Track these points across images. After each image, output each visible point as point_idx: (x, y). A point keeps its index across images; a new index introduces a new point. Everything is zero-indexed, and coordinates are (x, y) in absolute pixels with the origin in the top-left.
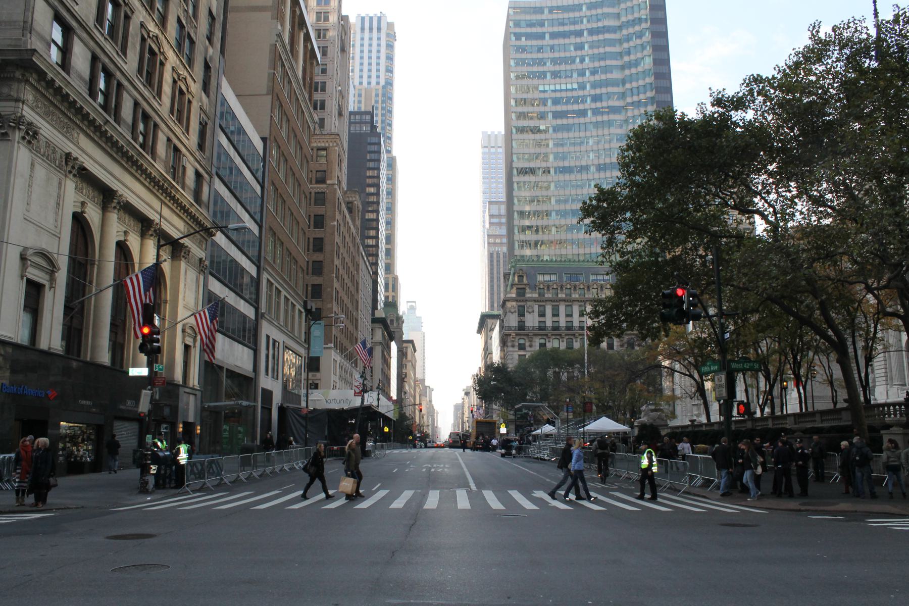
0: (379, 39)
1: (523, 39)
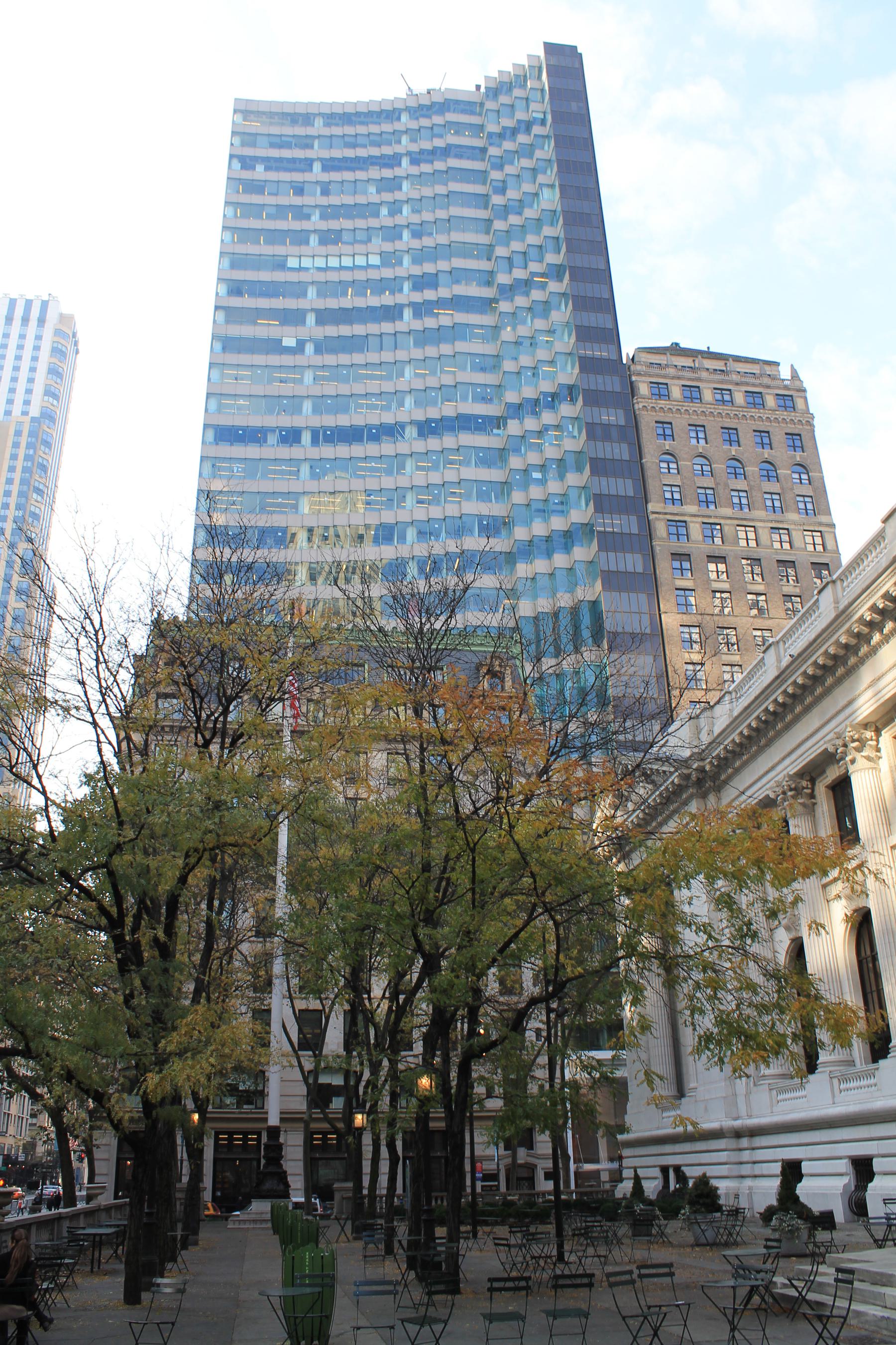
0: (39, 338)
1: (260, 168)
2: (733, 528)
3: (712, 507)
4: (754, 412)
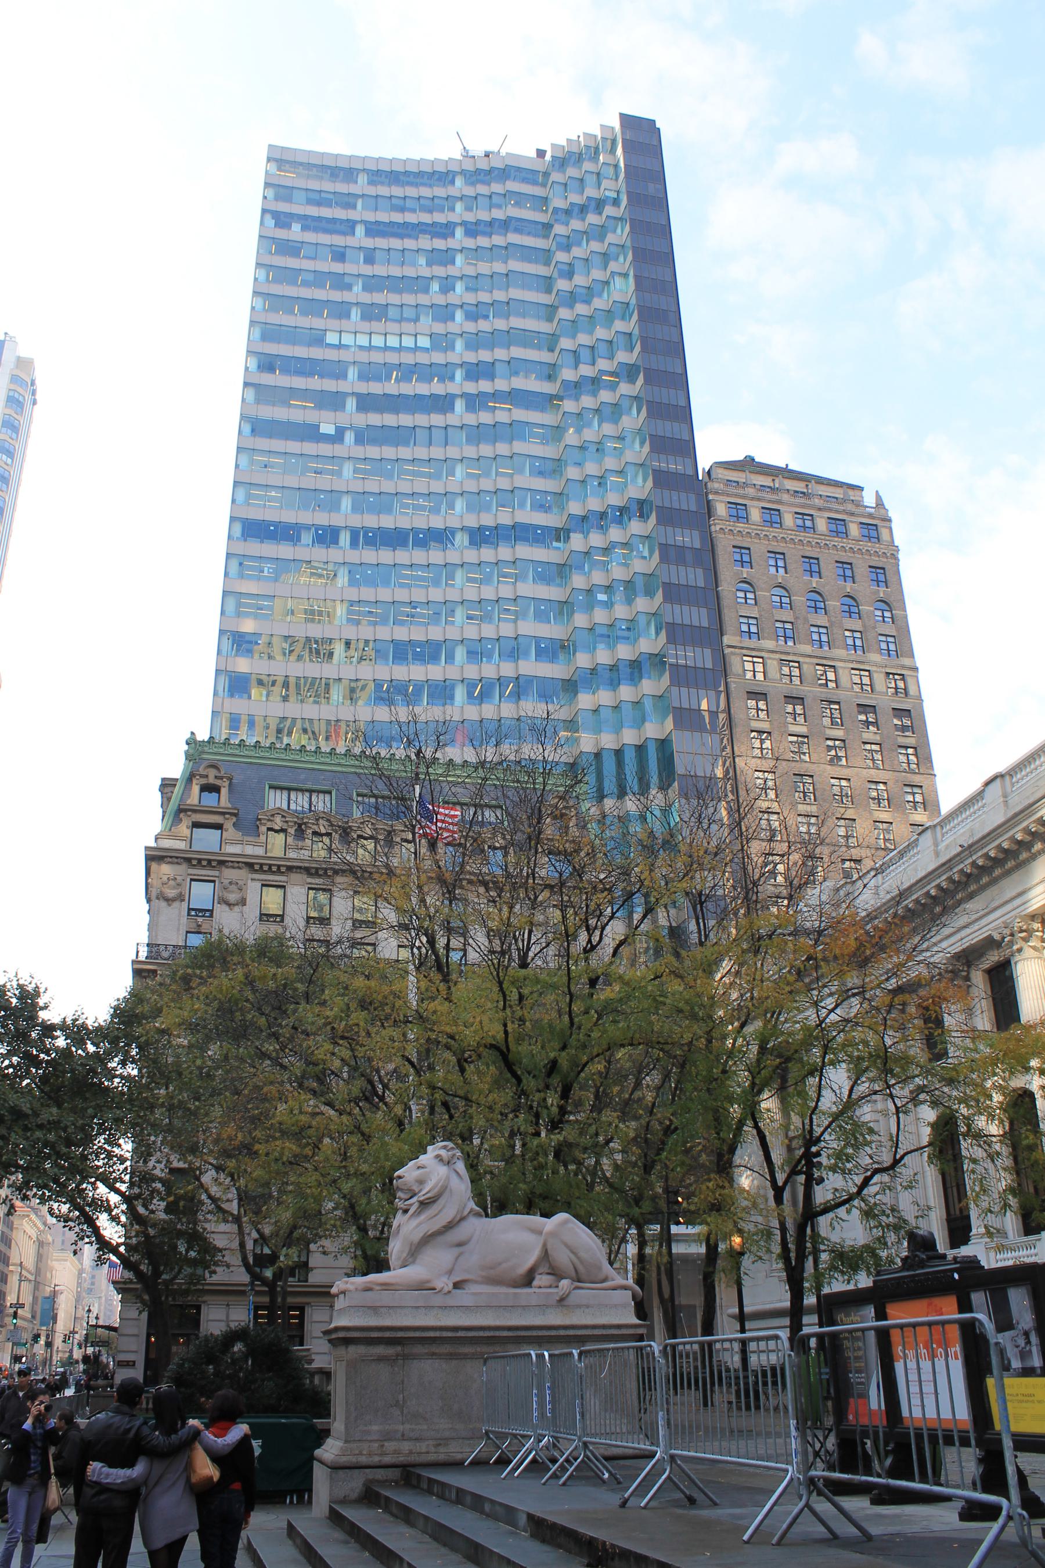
1: (296, 227)
2: (812, 667)
3: (790, 643)
4: (837, 541)
